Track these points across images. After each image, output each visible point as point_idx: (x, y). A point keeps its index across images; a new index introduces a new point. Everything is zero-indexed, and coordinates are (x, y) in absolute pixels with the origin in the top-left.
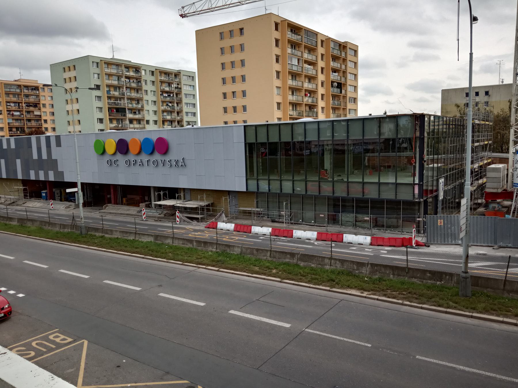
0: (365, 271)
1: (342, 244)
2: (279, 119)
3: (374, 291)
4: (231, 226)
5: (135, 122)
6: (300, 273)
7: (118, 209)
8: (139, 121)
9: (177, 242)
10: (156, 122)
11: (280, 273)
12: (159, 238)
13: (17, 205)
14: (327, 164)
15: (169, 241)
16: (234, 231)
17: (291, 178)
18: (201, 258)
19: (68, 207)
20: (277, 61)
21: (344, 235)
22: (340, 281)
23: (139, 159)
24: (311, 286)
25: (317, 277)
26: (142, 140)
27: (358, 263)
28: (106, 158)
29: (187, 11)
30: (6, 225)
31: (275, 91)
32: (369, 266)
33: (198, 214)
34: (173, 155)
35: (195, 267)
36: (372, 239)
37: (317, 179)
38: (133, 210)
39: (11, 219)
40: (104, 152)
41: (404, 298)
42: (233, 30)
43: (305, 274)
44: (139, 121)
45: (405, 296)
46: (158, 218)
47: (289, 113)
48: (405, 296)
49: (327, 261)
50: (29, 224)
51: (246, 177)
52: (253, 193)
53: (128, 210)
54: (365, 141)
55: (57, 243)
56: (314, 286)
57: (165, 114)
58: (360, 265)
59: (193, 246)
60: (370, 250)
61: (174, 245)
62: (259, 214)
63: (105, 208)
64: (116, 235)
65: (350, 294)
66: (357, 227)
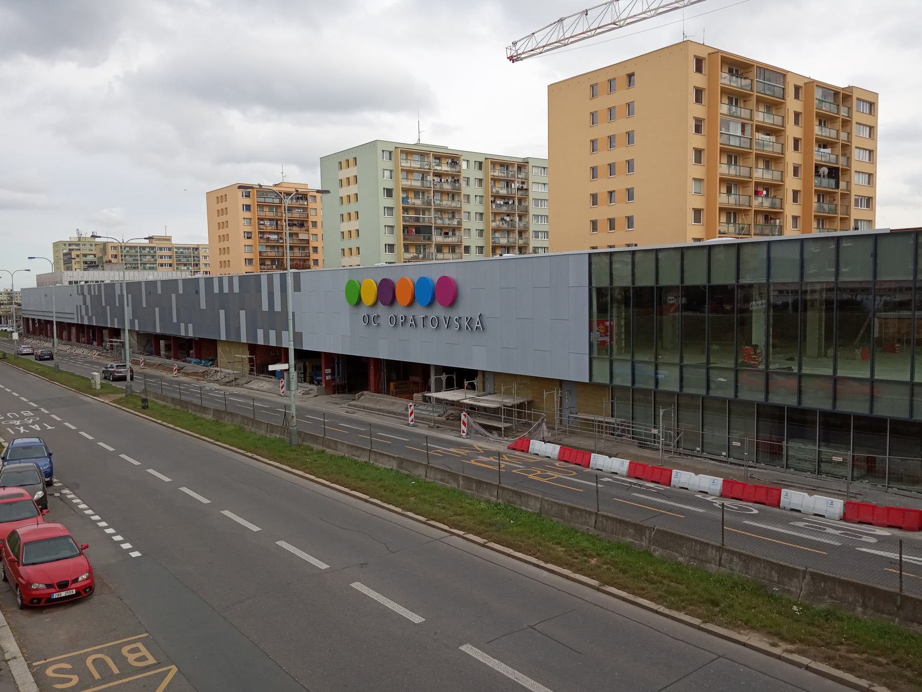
0: (798, 588)
1: (776, 510)
2: (695, 240)
3: (804, 643)
4: (553, 450)
5: (446, 250)
6: (647, 574)
7: (378, 401)
8: (453, 248)
9: (432, 476)
10: (481, 249)
11: (605, 567)
12: (405, 464)
13: (237, 385)
14: (758, 334)
15: (420, 472)
16: (559, 459)
17: (677, 361)
18: (462, 514)
19: (307, 393)
20: (698, 129)
21: (784, 491)
22: (730, 607)
23: (410, 314)
24: (661, 609)
25: (682, 588)
26: (416, 281)
27: (782, 567)
28: (363, 311)
29: (521, 48)
30: (195, 418)
31: (692, 186)
32: (808, 577)
33: (499, 420)
34: (464, 310)
35: (446, 531)
36: (846, 505)
37: (730, 363)
38: (397, 403)
39: (204, 409)
40: (359, 302)
41: (877, 674)
42: (614, 79)
43: (655, 578)
44: (453, 248)
45: (880, 669)
46: (436, 422)
47: (718, 228)
48: (880, 669)
49: (712, 553)
50: (227, 420)
51: (590, 354)
52: (601, 387)
53: (393, 404)
54: (839, 286)
55: (251, 457)
56: (667, 611)
57: (497, 235)
58: (787, 572)
59: (458, 485)
60: (838, 532)
61: (428, 480)
62: (612, 430)
63: (359, 398)
64: (343, 452)
65: (744, 645)
66: (818, 476)
